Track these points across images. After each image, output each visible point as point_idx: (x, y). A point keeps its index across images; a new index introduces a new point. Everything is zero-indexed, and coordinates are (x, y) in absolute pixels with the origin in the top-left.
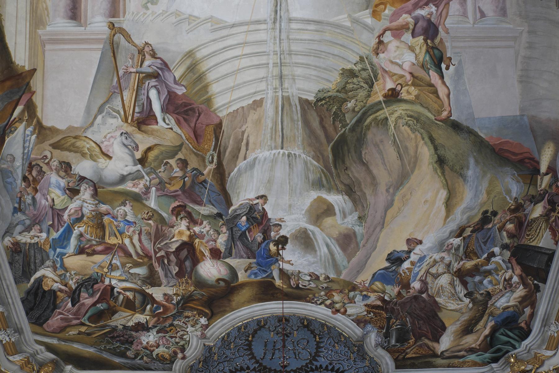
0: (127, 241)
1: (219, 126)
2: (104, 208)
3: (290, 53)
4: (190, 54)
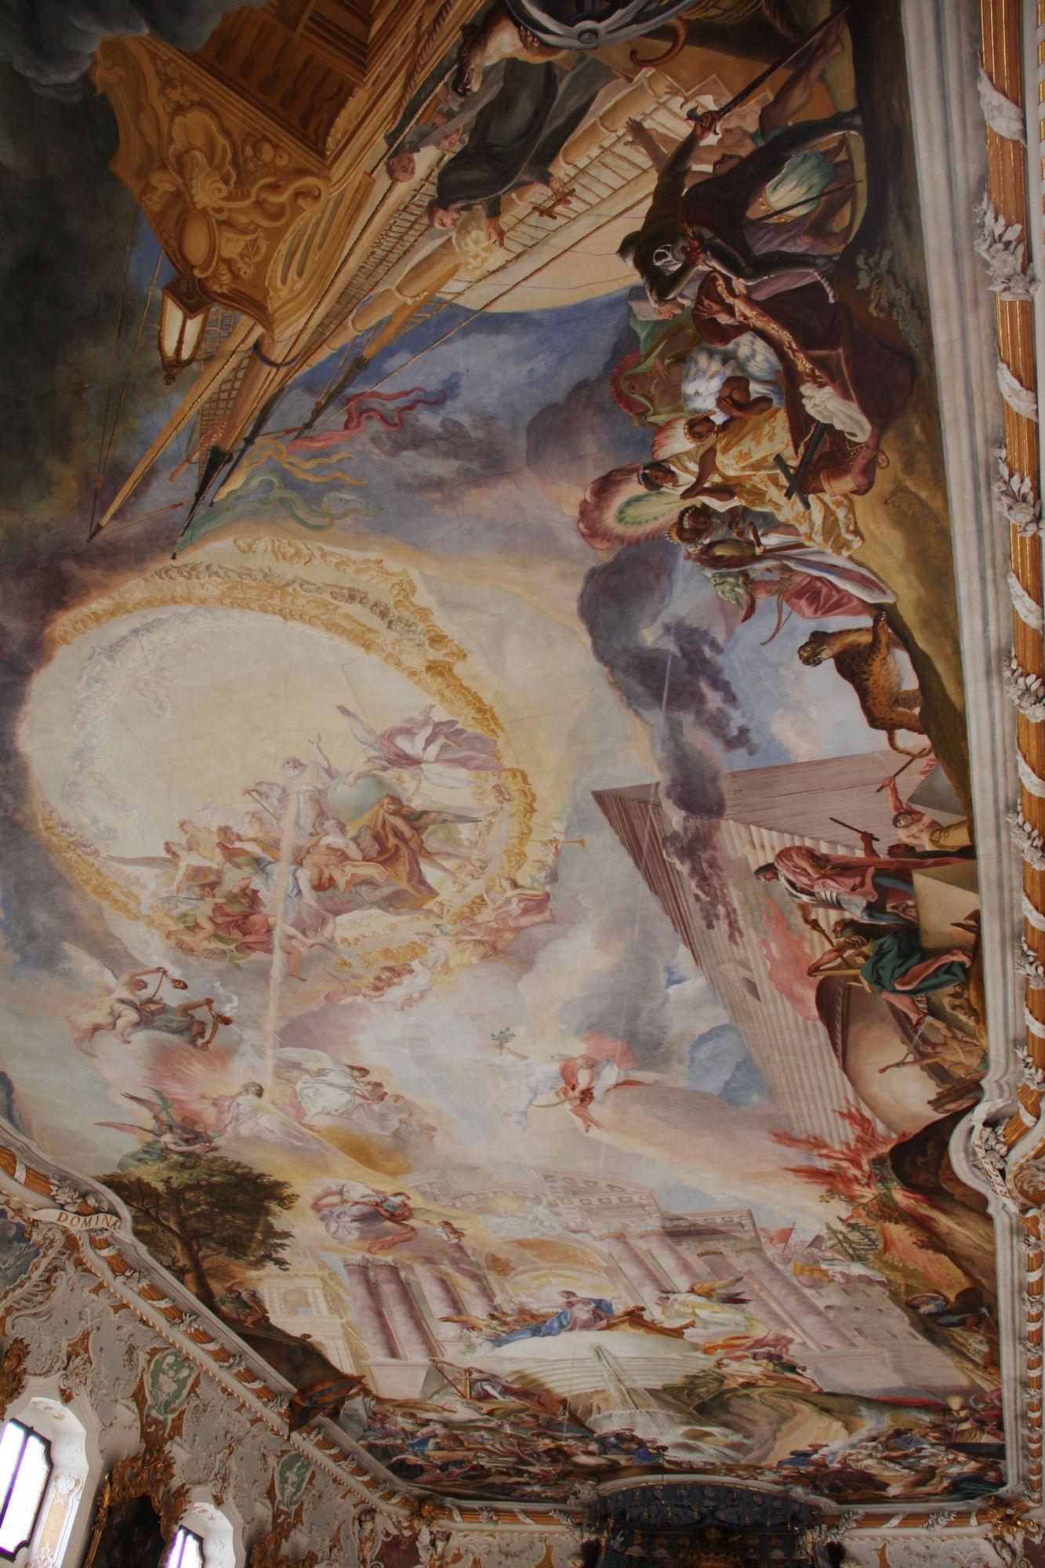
0: (489, 1447)
4: (517, 1372)
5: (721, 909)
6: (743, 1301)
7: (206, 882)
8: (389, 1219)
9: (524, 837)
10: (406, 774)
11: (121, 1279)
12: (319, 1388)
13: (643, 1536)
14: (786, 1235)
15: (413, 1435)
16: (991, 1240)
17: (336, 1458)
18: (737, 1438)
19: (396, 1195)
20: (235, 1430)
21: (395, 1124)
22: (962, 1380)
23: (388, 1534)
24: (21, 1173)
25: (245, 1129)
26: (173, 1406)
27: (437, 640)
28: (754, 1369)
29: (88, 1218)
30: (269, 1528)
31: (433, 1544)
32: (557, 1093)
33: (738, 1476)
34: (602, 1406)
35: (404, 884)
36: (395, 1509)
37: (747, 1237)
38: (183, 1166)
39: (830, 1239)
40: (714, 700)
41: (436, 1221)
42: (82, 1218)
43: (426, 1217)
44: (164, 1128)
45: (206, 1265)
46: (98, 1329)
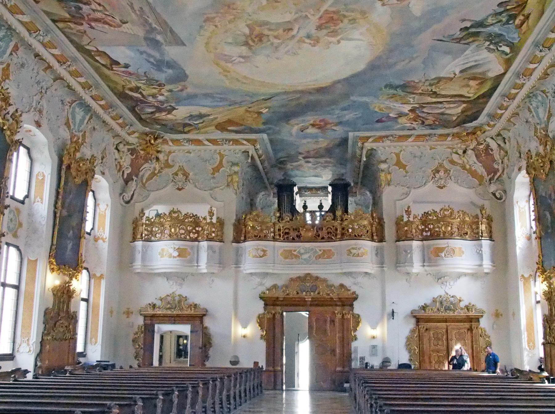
5: (138, 12)
7: (334, 33)
9: (210, 37)
10: (244, 55)
27: (226, 76)
35: (257, 29)
40: (152, 60)
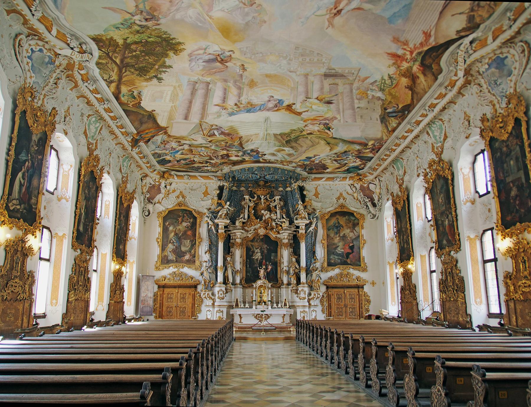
0: (202, 154)
1: (242, 137)
2: (192, 148)
3: (271, 127)
6: (331, 103)
8: (219, 62)
11: (86, 84)
12: (147, 131)
13: (237, 183)
14: (366, 78)
15: (174, 149)
16: (429, 88)
17: (141, 158)
18: (292, 151)
19: (229, 51)
20: (112, 148)
21: (249, 18)
22: (379, 136)
23: (151, 184)
24: (54, 32)
25: (178, 16)
26: (94, 138)
28: (316, 128)
29: (83, 55)
30: (121, 182)
31: (166, 187)
32: (327, 10)
33: (283, 165)
34: (253, 140)
36: (155, 175)
37: (351, 78)
38: (138, 32)
39: (379, 82)
41: (239, 64)
42: (80, 55)
43: (234, 62)
44: (139, 12)
45: (124, 79)
46: (72, 106)
